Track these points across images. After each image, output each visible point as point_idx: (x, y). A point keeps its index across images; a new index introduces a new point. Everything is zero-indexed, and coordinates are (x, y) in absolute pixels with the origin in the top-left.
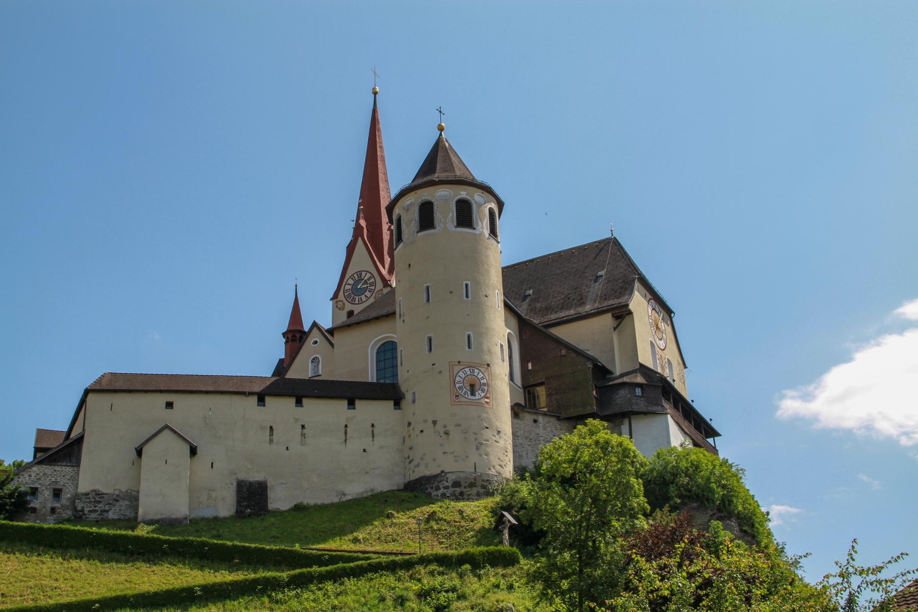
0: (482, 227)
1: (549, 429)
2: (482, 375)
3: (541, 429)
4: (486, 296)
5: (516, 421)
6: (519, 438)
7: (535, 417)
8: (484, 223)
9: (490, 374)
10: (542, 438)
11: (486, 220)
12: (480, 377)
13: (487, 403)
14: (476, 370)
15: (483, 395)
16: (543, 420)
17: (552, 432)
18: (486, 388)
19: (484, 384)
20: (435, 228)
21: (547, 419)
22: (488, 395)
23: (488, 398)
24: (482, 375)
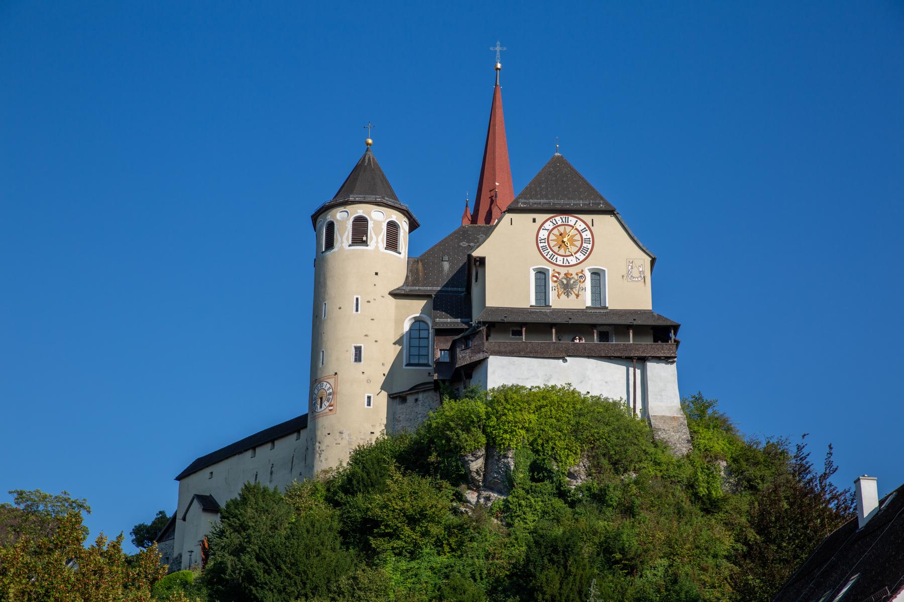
0: (342, 242)
1: (426, 404)
2: (328, 386)
3: (420, 406)
4: (340, 308)
5: (400, 408)
6: (401, 422)
7: (415, 396)
8: (345, 237)
9: (336, 382)
10: (420, 416)
11: (347, 233)
12: (326, 389)
13: (331, 410)
14: (325, 383)
15: (327, 404)
16: (423, 397)
17: (430, 405)
18: (331, 397)
19: (330, 394)
20: (368, 246)
21: (426, 395)
22: (332, 403)
23: (332, 406)
24: (328, 386)
